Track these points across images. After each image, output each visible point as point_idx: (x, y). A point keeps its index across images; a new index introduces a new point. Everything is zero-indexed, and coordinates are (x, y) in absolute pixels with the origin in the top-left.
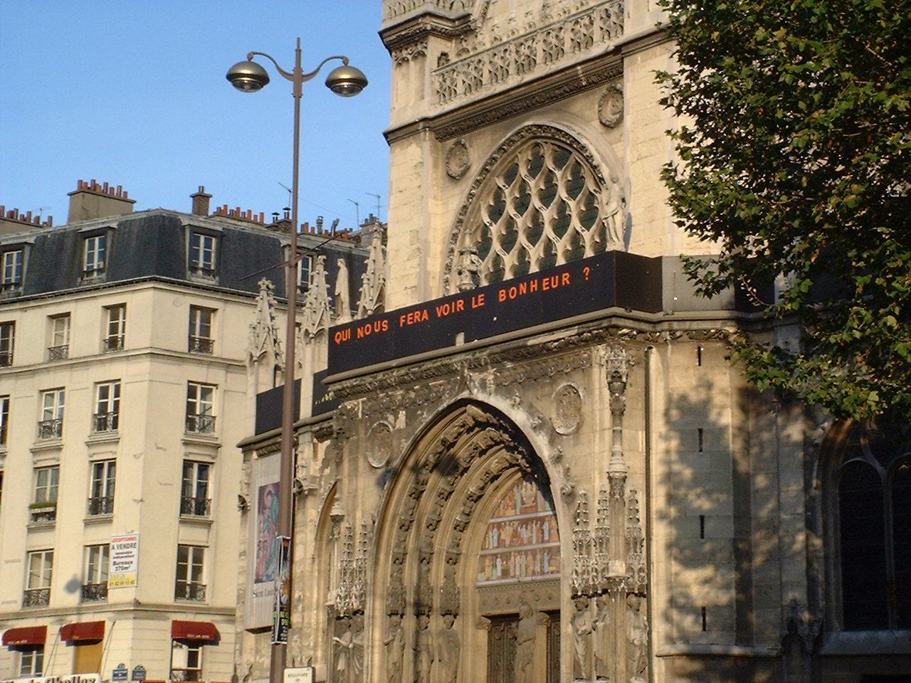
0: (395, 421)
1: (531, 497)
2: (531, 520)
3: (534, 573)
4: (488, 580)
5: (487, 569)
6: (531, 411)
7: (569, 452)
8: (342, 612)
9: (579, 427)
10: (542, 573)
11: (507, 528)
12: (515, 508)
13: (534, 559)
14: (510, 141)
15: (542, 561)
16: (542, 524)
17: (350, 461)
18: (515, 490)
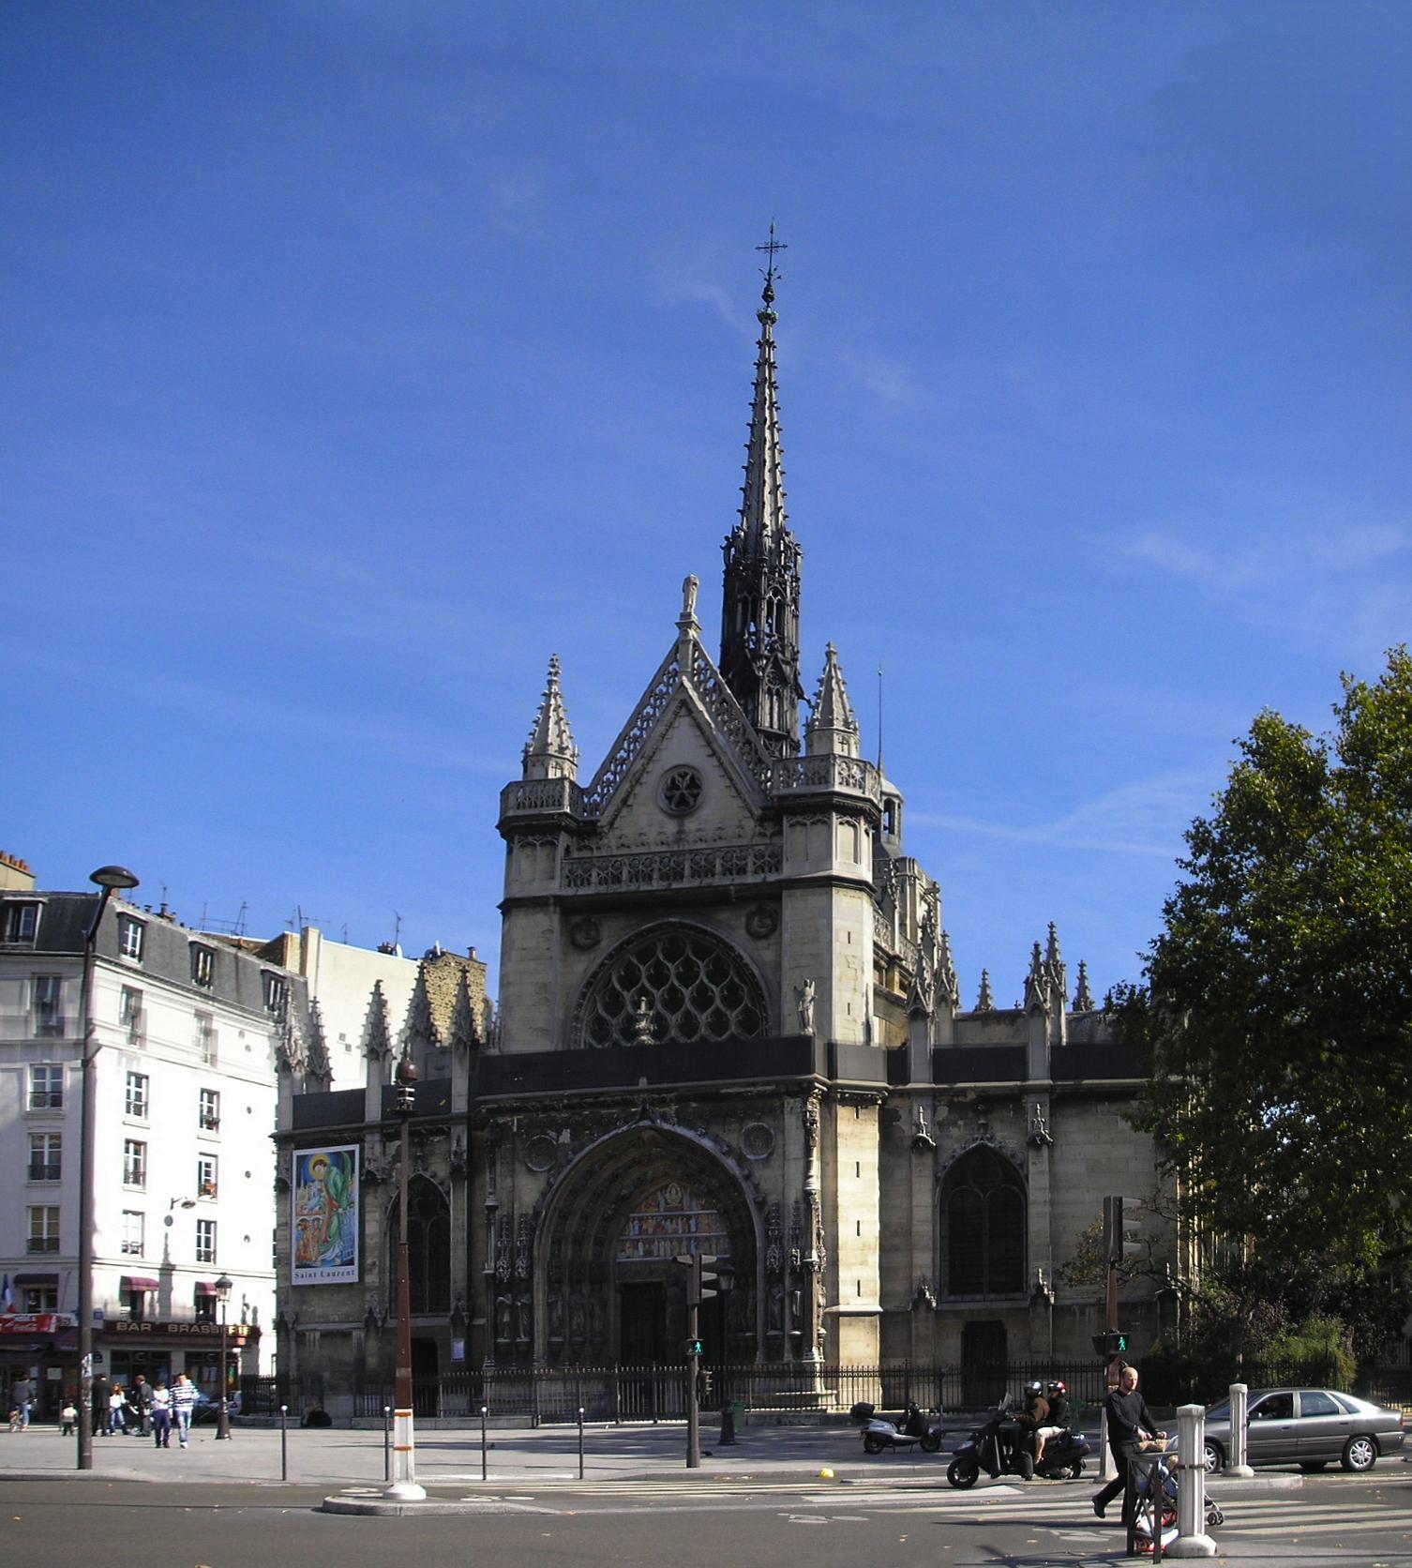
0: (559, 1134)
6: (716, 1139)
7: (759, 1173)
9: (770, 1155)
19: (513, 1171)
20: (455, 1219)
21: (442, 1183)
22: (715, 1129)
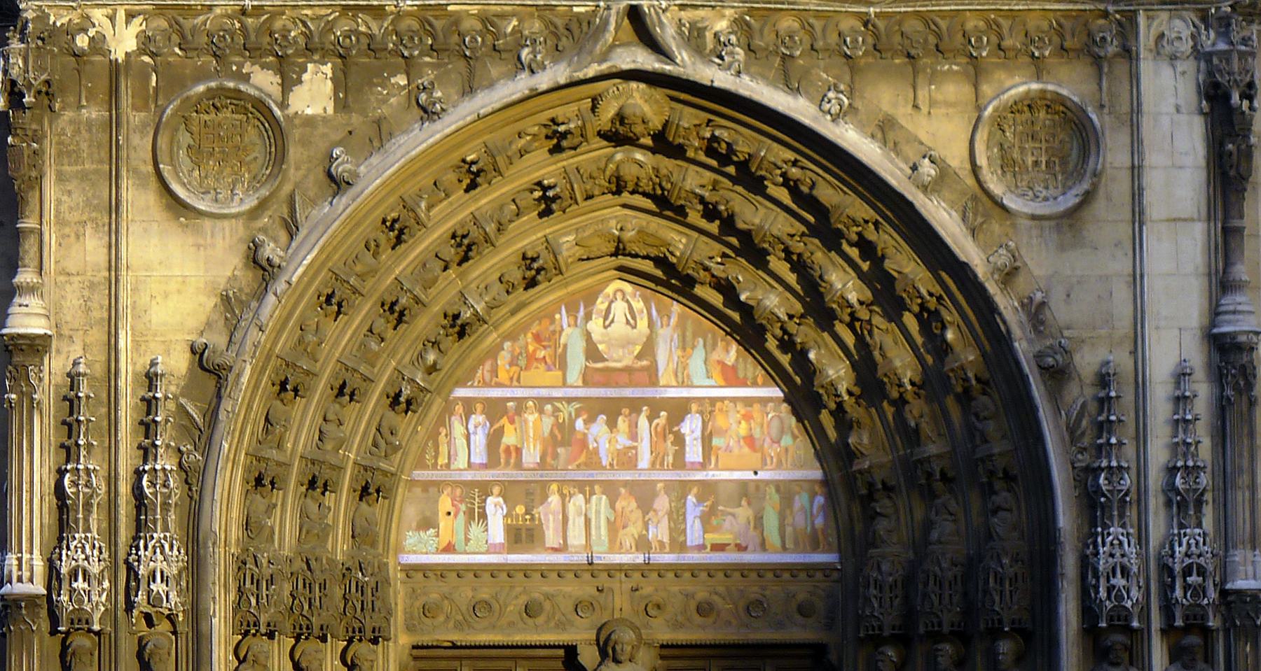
1: (627, 343)
2: (635, 405)
3: (642, 544)
4: (450, 548)
5: (443, 522)
6: (885, 130)
8: (97, 617)
9: (1088, 198)
11: (531, 417)
12: (563, 366)
13: (646, 506)
15: (677, 518)
17: (61, 178)
19: (114, 208)
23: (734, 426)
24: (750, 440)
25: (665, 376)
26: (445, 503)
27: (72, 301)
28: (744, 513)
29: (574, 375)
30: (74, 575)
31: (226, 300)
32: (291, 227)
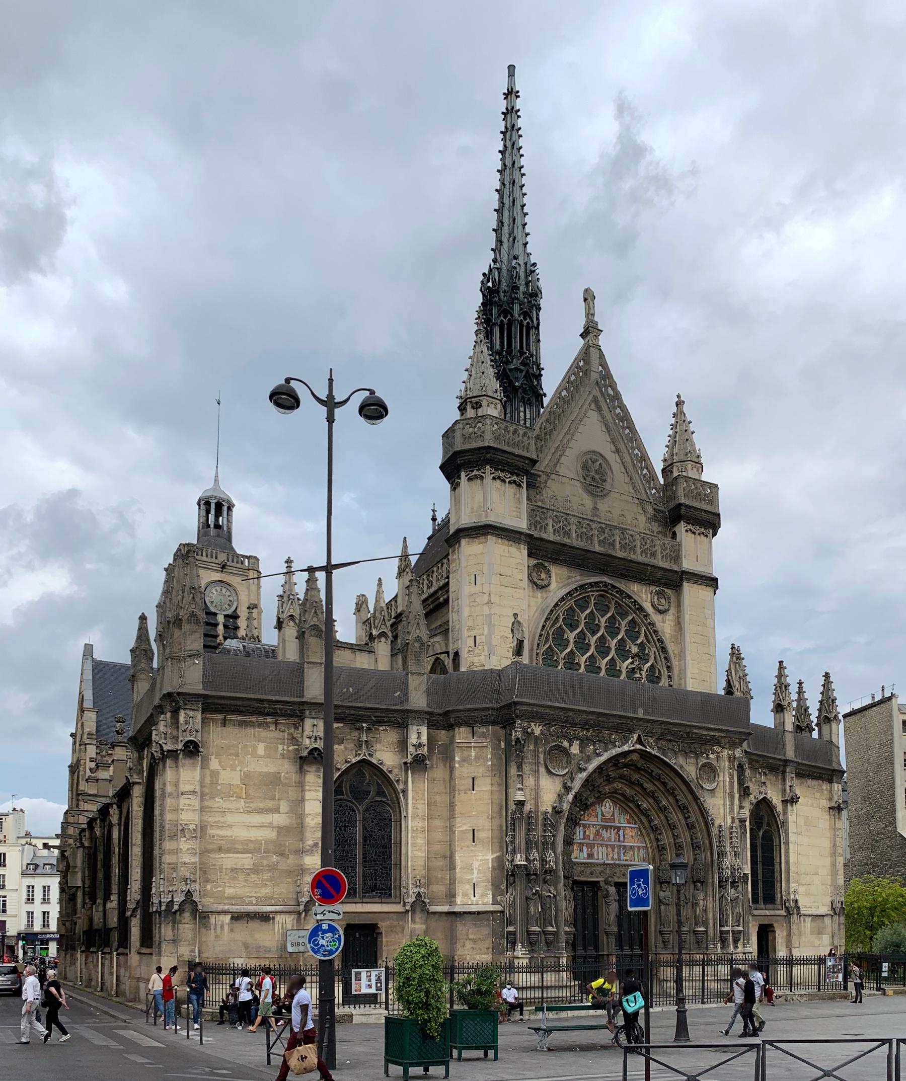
0: (570, 747)
1: (609, 813)
2: (611, 827)
3: (613, 859)
10: (619, 860)
13: (613, 850)
14: (591, 585)
15: (619, 853)
16: (618, 831)
18: (597, 806)
19: (537, 772)
20: (415, 808)
21: (390, 772)
22: (681, 760)
23: (629, 833)
24: (632, 836)
25: (616, 821)
26: (575, 847)
27: (528, 793)
28: (631, 853)
29: (599, 820)
30: (534, 860)
31: (559, 795)
32: (572, 779)
